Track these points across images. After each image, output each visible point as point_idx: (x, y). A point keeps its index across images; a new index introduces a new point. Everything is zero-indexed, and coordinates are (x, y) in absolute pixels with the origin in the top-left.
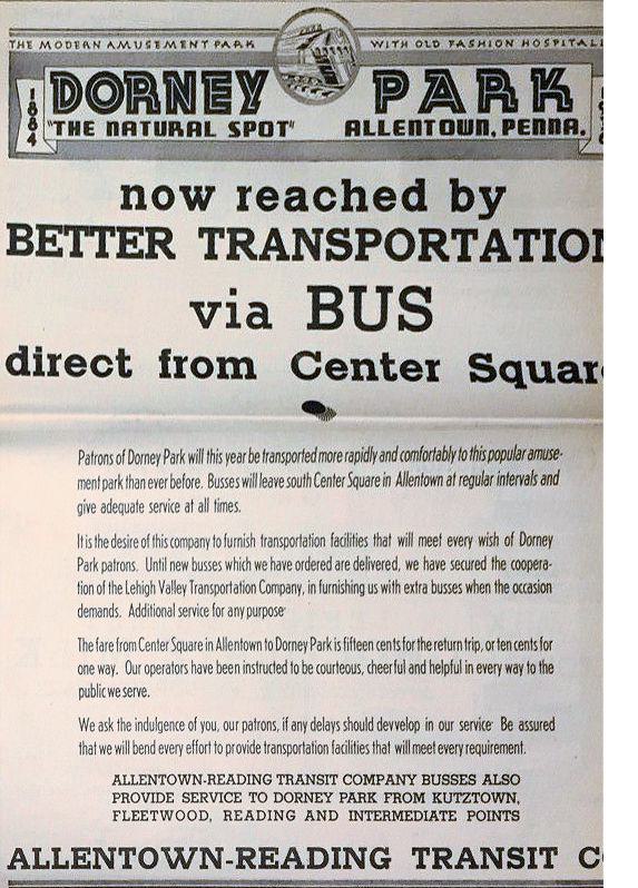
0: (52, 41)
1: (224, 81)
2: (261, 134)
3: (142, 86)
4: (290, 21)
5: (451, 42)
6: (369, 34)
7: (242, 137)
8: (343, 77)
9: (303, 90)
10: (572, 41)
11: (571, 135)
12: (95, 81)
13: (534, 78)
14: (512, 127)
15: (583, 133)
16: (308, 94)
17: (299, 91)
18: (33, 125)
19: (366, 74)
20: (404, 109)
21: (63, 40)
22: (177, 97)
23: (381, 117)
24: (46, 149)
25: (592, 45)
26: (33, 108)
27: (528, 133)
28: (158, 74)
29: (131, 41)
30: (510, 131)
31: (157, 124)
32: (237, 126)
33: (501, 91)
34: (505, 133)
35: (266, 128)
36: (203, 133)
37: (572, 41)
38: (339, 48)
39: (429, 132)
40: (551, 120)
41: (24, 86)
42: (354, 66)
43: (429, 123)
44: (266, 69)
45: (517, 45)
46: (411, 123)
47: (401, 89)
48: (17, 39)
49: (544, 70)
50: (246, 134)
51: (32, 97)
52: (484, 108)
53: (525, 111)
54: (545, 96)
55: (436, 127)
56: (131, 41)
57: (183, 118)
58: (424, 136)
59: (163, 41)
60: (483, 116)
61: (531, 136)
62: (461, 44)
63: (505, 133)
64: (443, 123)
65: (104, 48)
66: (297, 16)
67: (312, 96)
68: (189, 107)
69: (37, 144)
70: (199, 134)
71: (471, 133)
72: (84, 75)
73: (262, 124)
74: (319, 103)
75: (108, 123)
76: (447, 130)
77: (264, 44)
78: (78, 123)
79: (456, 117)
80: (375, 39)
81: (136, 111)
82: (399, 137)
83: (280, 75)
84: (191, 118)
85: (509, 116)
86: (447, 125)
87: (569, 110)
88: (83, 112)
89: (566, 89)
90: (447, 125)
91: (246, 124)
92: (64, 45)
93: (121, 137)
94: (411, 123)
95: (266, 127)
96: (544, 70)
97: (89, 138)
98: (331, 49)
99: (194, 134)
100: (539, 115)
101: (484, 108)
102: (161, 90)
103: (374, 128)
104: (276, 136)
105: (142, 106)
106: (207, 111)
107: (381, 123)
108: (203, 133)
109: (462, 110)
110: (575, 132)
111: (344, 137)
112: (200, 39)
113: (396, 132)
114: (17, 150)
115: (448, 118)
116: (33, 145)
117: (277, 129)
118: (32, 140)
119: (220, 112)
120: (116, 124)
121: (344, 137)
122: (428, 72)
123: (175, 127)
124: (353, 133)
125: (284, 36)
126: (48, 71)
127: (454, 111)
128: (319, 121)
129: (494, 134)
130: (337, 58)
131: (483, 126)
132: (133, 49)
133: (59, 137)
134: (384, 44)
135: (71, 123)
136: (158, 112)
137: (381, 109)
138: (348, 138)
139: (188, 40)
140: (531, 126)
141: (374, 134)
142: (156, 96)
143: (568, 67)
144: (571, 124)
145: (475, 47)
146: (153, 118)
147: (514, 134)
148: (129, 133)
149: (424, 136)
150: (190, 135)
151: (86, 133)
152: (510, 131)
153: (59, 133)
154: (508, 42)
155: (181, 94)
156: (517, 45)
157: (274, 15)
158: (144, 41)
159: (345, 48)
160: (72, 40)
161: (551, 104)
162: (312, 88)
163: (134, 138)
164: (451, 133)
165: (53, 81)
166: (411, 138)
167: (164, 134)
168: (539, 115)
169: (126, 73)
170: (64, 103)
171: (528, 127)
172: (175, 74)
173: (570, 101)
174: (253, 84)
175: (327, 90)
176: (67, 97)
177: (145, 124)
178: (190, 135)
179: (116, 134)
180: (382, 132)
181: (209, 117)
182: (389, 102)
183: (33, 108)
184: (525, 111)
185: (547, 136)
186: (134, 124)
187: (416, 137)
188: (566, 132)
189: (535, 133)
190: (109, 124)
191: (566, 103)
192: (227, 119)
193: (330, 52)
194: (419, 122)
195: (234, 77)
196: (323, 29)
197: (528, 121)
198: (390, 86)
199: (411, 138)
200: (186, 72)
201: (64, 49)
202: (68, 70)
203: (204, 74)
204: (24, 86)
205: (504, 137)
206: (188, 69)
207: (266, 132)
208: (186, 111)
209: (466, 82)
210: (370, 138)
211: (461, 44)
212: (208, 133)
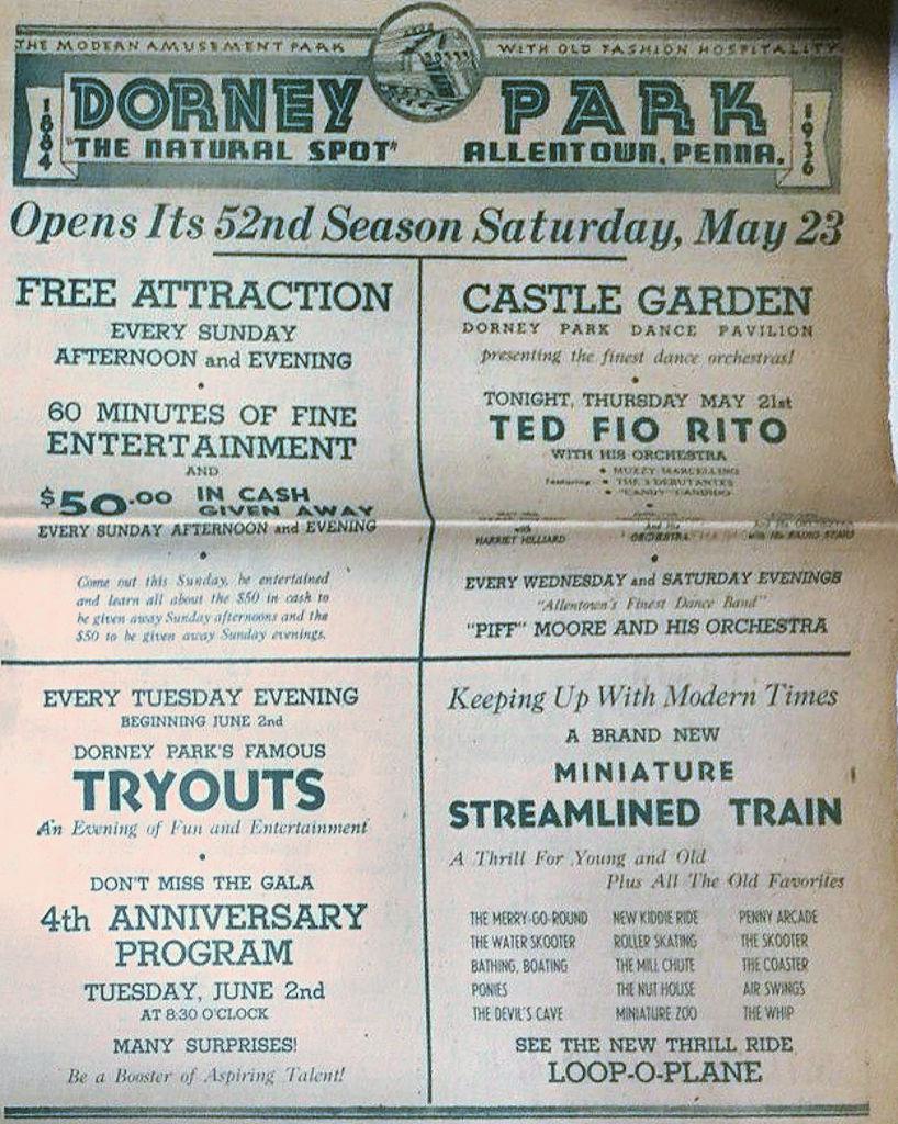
0: (74, 40)
1: (302, 92)
2: (353, 156)
3: (193, 96)
4: (391, 19)
7: (327, 161)
9: (409, 103)
12: (132, 90)
13: (715, 95)
15: (781, 161)
18: (47, 143)
19: (491, 87)
20: (545, 128)
21: (89, 40)
22: (241, 112)
23: (512, 138)
24: (67, 175)
26: (47, 122)
27: (708, 161)
28: (215, 82)
30: (684, 158)
32: (320, 147)
33: (671, 109)
34: (678, 159)
35: (359, 148)
36: (275, 154)
39: (577, 158)
40: (738, 147)
41: (35, 95)
46: (553, 146)
48: (27, 38)
50: (333, 157)
51: (47, 108)
52: (649, 128)
53: (704, 132)
55: (586, 152)
59: (221, 44)
60: (647, 139)
61: (712, 164)
62: (618, 49)
63: (678, 159)
64: (595, 146)
65: (143, 49)
66: (405, 10)
67: (420, 111)
68: (257, 124)
70: (269, 157)
71: (632, 159)
72: (116, 82)
73: (354, 145)
76: (601, 155)
77: (359, 48)
78: (107, 141)
80: (504, 42)
81: (185, 128)
83: (376, 86)
84: (259, 136)
88: (115, 127)
89: (757, 108)
90: (601, 149)
91: (333, 144)
93: (164, 158)
94: (553, 146)
95: (360, 148)
96: (728, 84)
97: (120, 160)
98: (446, 54)
100: (721, 139)
101: (649, 128)
102: (219, 102)
103: (503, 151)
104: (373, 160)
105: (194, 120)
106: (280, 128)
107: (513, 147)
108: (275, 154)
109: (622, 132)
110: (771, 160)
111: (459, 160)
113: (533, 157)
115: (604, 141)
116: (46, 169)
117: (374, 151)
118: (45, 162)
119: (298, 130)
120: (158, 143)
121: (462, 163)
124: (475, 158)
126: (67, 78)
127: (610, 132)
128: (428, 143)
129: (663, 161)
130: (455, 67)
131: (648, 151)
135: (97, 141)
137: (512, 128)
141: (503, 160)
142: (213, 110)
143: (757, 79)
145: (637, 54)
146: (207, 136)
148: (176, 154)
149: (570, 162)
150: (257, 156)
151: (118, 153)
152: (684, 158)
153: (82, 152)
155: (245, 107)
158: (197, 41)
161: (737, 126)
162: (422, 101)
164: (607, 158)
165: (73, 89)
166: (553, 164)
167: (222, 155)
168: (721, 139)
169: (172, 81)
170: (88, 116)
171: (707, 153)
172: (238, 82)
173: (762, 123)
174: (342, 98)
175: (440, 104)
176: (93, 109)
177: (198, 144)
178: (257, 156)
180: (513, 155)
181: (282, 136)
182: (525, 122)
183: (47, 122)
184: (704, 132)
185: (734, 164)
186: (182, 143)
187: (559, 164)
188: (759, 160)
189: (717, 160)
190: (149, 143)
191: (756, 124)
192: (307, 138)
193: (445, 58)
194: (563, 145)
195: (316, 84)
196: (436, 28)
198: (524, 101)
199: (553, 164)
200: (252, 81)
201: (89, 51)
202: (94, 75)
203: (275, 80)
204: (35, 95)
207: (359, 154)
208: (251, 127)
209: (625, 97)
211: (618, 49)
212: (281, 155)
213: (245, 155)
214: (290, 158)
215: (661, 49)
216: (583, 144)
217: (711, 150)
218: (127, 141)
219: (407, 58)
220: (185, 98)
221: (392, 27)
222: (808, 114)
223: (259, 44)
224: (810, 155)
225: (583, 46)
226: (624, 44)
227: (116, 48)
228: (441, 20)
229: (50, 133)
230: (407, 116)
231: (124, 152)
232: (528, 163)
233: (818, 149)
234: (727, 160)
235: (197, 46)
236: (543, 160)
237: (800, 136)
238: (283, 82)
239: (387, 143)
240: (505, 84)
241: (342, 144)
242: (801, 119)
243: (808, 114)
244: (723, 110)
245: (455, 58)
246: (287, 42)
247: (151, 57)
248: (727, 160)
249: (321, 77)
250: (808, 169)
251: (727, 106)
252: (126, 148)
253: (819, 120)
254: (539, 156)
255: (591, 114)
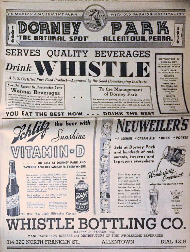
0: (19, 13)
1: (68, 25)
2: (79, 40)
3: (44, 26)
5: (134, 14)
6: (111, 12)
7: (73, 41)
8: (103, 24)
9: (91, 27)
10: (169, 13)
11: (169, 41)
12: (31, 25)
13: (158, 25)
14: (152, 39)
15: (172, 40)
16: (92, 29)
17: (90, 28)
18: (13, 36)
19: (109, 23)
20: (121, 33)
21: (22, 13)
23: (114, 35)
25: (175, 15)
26: (13, 32)
28: (49, 23)
29: (41, 13)
31: (49, 37)
33: (148, 28)
34: (149, 40)
35: (80, 38)
37: (169, 13)
38: (101, 16)
39: (128, 40)
41: (10, 26)
42: (106, 20)
43: (128, 37)
44: (80, 21)
45: (153, 15)
46: (122, 37)
47: (119, 28)
48: (8, 12)
49: (161, 22)
50: (75, 40)
51: (13, 28)
52: (143, 33)
53: (155, 34)
54: (161, 30)
55: (129, 39)
56: (41, 13)
57: (56, 35)
58: (126, 41)
59: (50, 13)
62: (137, 14)
63: (149, 40)
64: (131, 37)
65: (33, 15)
67: (94, 29)
68: (58, 32)
69: (14, 42)
70: (61, 40)
71: (139, 40)
72: (28, 23)
73: (79, 37)
74: (96, 31)
75: (35, 36)
76: (133, 39)
77: (80, 14)
78: (26, 36)
79: (135, 36)
80: (112, 13)
81: (43, 33)
82: (119, 41)
83: (84, 23)
85: (150, 35)
86: (133, 38)
87: (168, 34)
88: (27, 33)
89: (167, 28)
90: (133, 38)
91: (75, 37)
92: (22, 14)
93: (38, 40)
94: (122, 37)
96: (161, 22)
97: (29, 40)
99: (60, 40)
100: (159, 35)
101: (143, 33)
102: (50, 27)
103: (111, 39)
105: (45, 32)
106: (63, 33)
107: (114, 37)
110: (170, 40)
111: (102, 40)
112: (61, 13)
113: (118, 40)
114: (8, 44)
115: (133, 36)
116: (13, 42)
117: (83, 39)
118: (13, 41)
120: (37, 37)
122: (127, 23)
123: (54, 38)
125: (85, 12)
126: (17, 21)
127: (135, 34)
128: (96, 37)
130: (101, 19)
131: (143, 38)
132: (42, 15)
133: (20, 40)
134: (115, 15)
135: (24, 36)
136: (49, 33)
137: (113, 33)
138: (104, 41)
139: (58, 13)
140: (157, 38)
141: (111, 40)
142: (49, 29)
143: (168, 21)
144: (169, 38)
145: (141, 15)
146: (48, 35)
147: (152, 40)
148: (41, 39)
149: (126, 41)
150: (58, 40)
151: (28, 39)
153: (20, 39)
154: (150, 14)
155: (56, 29)
156: (153, 15)
157: (83, 6)
159: (103, 16)
160: (24, 13)
161: (163, 32)
163: (42, 41)
164: (134, 40)
166: (122, 41)
168: (159, 35)
169: (40, 22)
170: (22, 30)
171: (156, 38)
172: (54, 23)
173: (168, 31)
174: (76, 26)
175: (98, 28)
177: (45, 37)
178: (58, 40)
179: (37, 39)
180: (114, 40)
181: (64, 35)
182: (116, 31)
183: (13, 32)
184: (155, 34)
186: (42, 37)
187: (123, 41)
189: (158, 40)
190: (35, 37)
191: (167, 32)
193: (99, 17)
194: (125, 37)
195: (71, 24)
197: (156, 37)
198: (116, 27)
199: (122, 41)
200: (57, 22)
201: (22, 15)
203: (62, 23)
204: (10, 26)
205: (149, 41)
206: (59, 21)
207: (80, 39)
208: (57, 33)
210: (111, 41)
211: (137, 14)
212: (63, 40)
213: (56, 40)
214: (65, 40)
215: (146, 14)
216: (129, 37)
217: (157, 38)
218: (30, 36)
219: (91, 17)
220: (42, 27)
221: (87, 10)
222: (178, 29)
223: (59, 14)
224: (178, 39)
225: (129, 14)
226: (138, 13)
227: (28, 14)
228: (98, 8)
229: (14, 34)
230: (90, 30)
231: (30, 39)
232: (117, 41)
233: (180, 37)
234: (160, 40)
235: (45, 15)
236: (120, 40)
237: (176, 34)
238: (64, 23)
239: (86, 37)
240: (112, 23)
241: (77, 37)
242: (176, 30)
243: (178, 29)
244: (160, 28)
245: (101, 17)
246: (65, 13)
247: (36, 17)
248: (160, 40)
249: (73, 21)
250: (178, 42)
251: (161, 27)
252: (30, 38)
253: (180, 31)
254: (119, 40)
255: (131, 30)
